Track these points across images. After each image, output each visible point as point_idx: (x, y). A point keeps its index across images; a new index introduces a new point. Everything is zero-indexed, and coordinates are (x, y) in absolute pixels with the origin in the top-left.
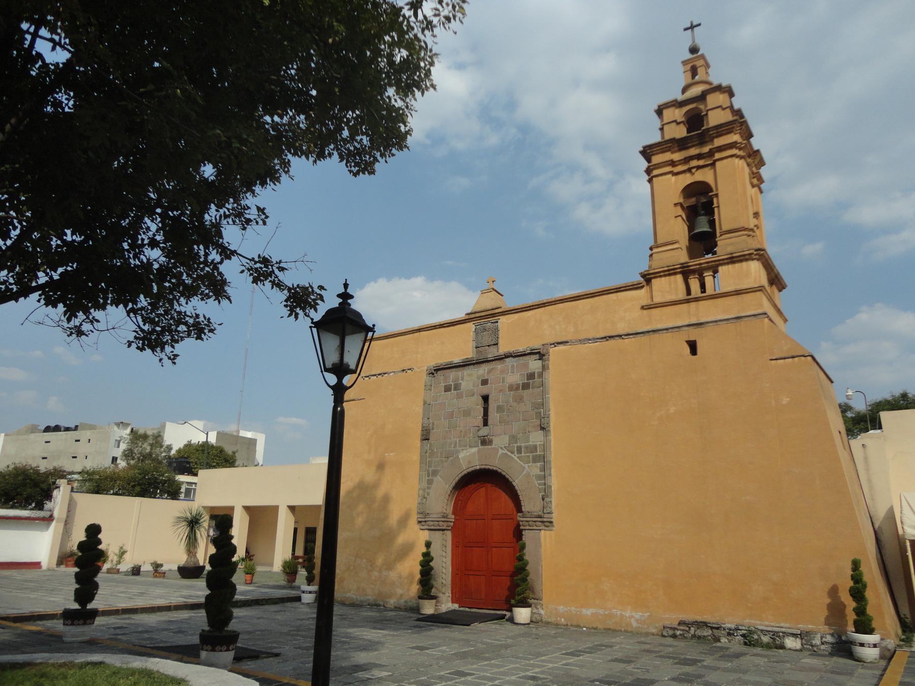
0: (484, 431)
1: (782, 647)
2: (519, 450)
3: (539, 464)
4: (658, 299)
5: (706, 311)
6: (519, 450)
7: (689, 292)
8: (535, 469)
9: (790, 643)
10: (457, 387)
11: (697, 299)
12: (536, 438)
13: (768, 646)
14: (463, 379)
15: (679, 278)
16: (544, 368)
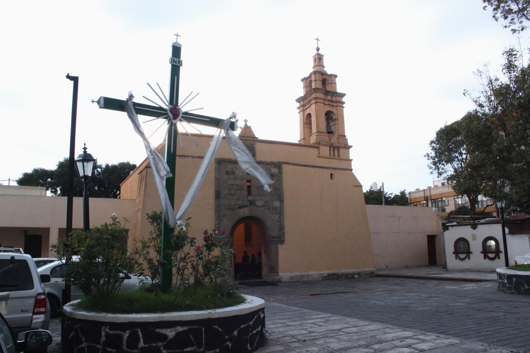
0: (250, 198)
1: (354, 278)
2: (269, 209)
3: (278, 216)
4: (322, 154)
5: (335, 163)
6: (269, 209)
7: (330, 155)
8: (276, 218)
9: (356, 276)
10: (233, 173)
11: (332, 158)
12: (277, 204)
13: (351, 278)
14: (236, 169)
15: (328, 148)
16: (280, 172)
